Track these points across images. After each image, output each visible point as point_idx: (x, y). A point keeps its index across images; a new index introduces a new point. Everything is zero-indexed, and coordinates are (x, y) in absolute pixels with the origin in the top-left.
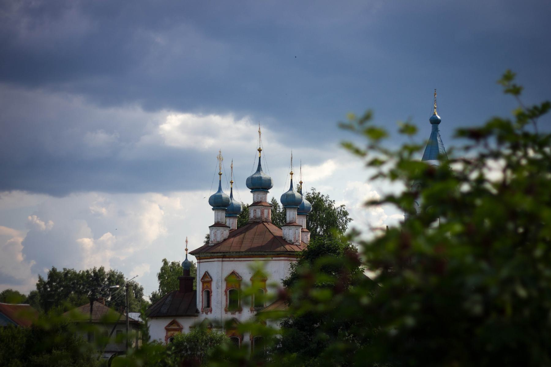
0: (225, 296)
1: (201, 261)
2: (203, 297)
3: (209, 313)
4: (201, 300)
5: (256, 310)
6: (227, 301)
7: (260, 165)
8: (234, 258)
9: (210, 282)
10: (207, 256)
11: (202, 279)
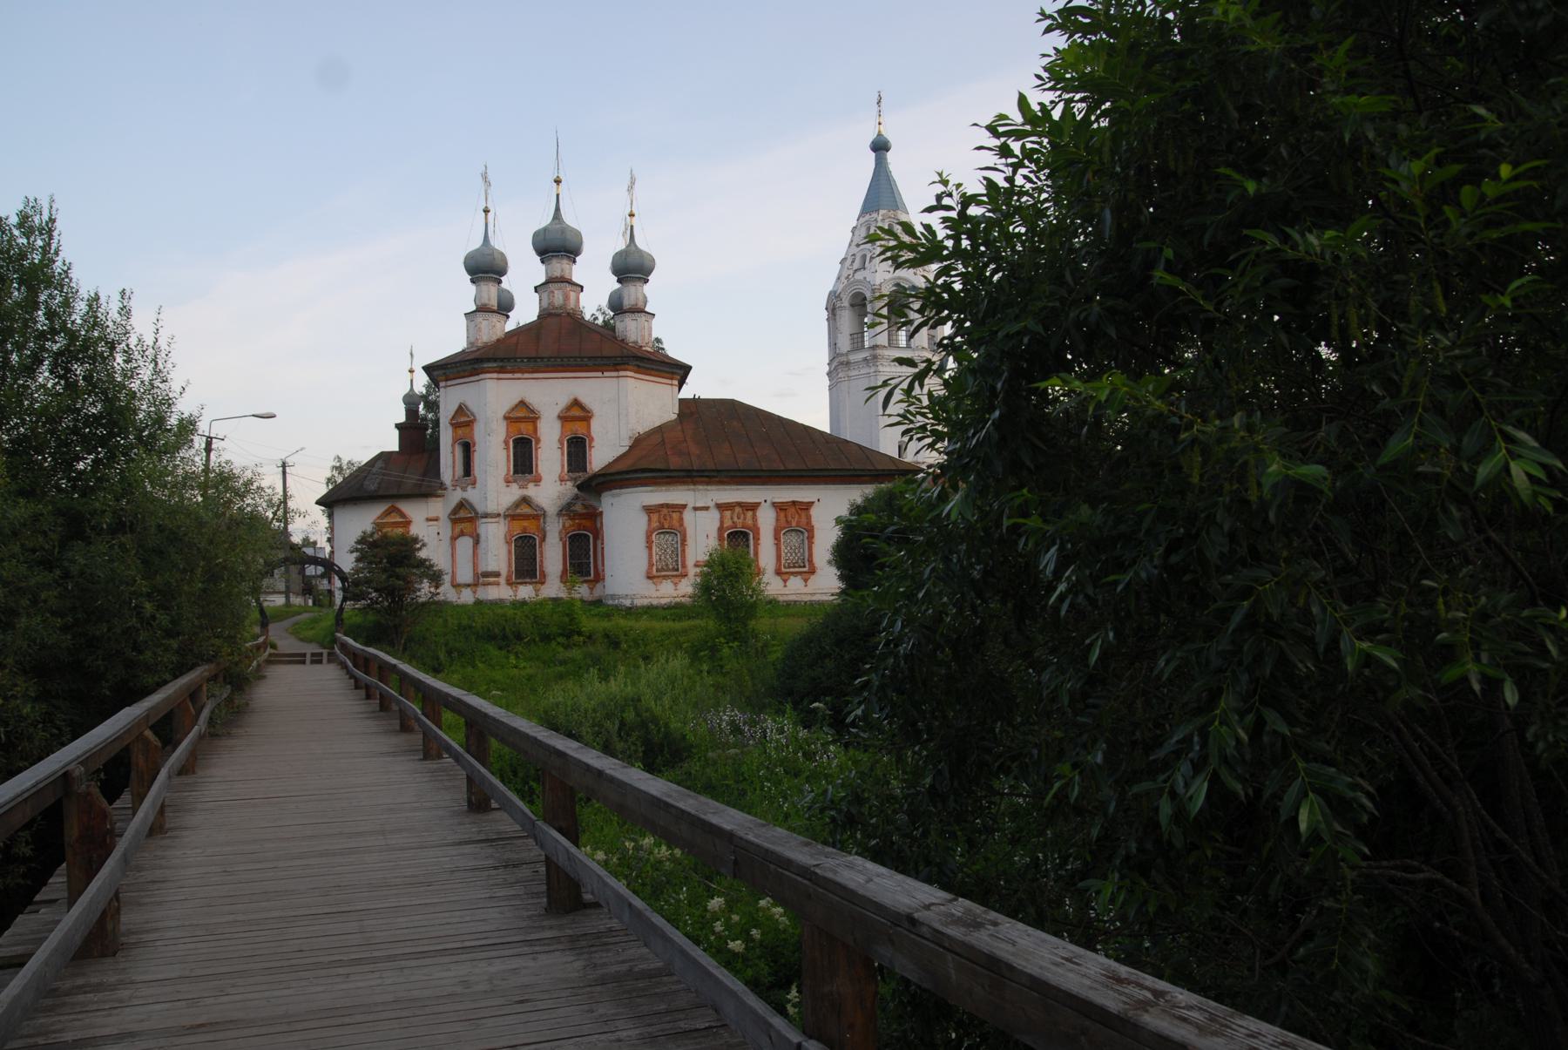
0: (505, 451)
1: (449, 383)
2: (454, 456)
3: (469, 488)
4: (450, 462)
5: (571, 479)
6: (508, 460)
7: (557, 209)
8: (523, 372)
9: (469, 424)
10: (464, 371)
11: (453, 418)
